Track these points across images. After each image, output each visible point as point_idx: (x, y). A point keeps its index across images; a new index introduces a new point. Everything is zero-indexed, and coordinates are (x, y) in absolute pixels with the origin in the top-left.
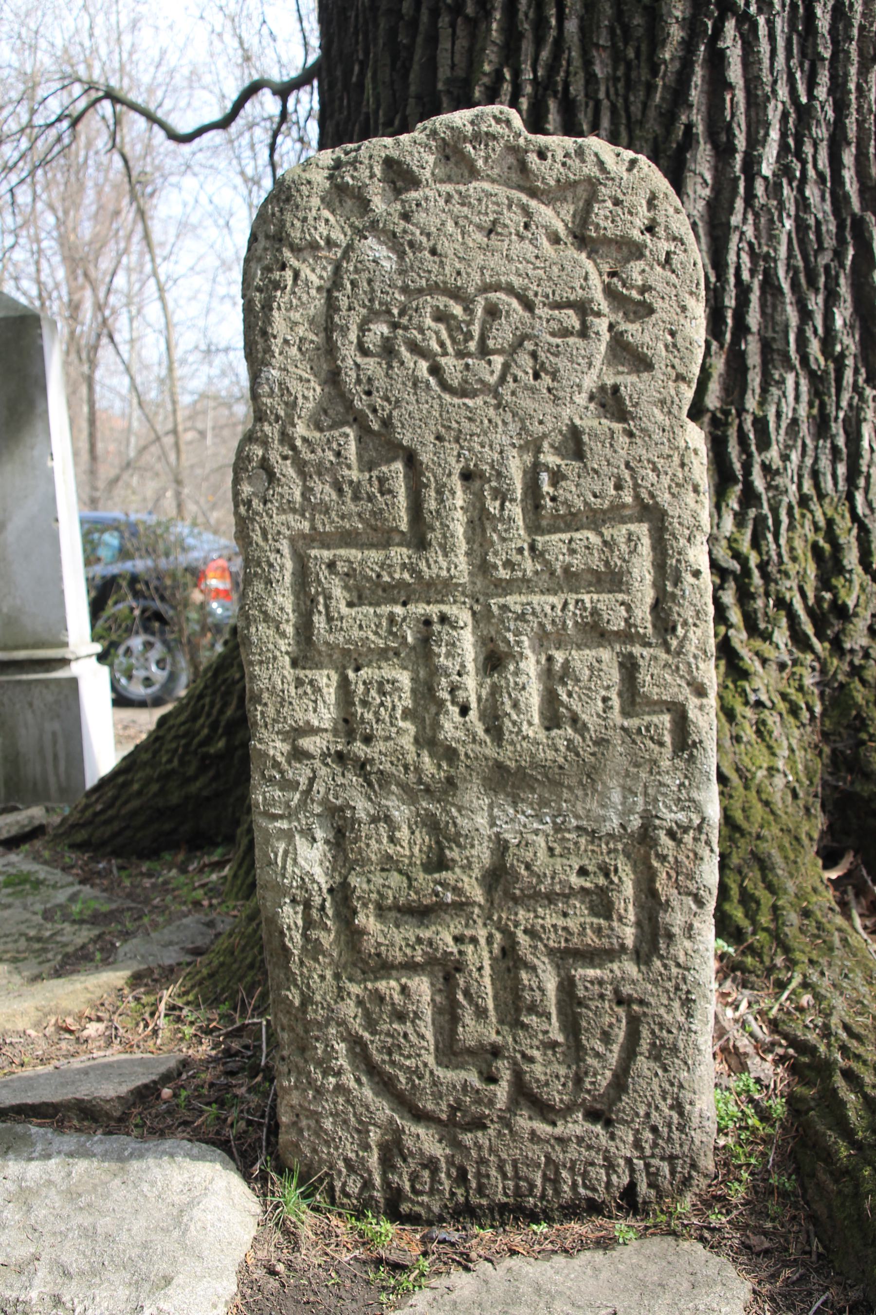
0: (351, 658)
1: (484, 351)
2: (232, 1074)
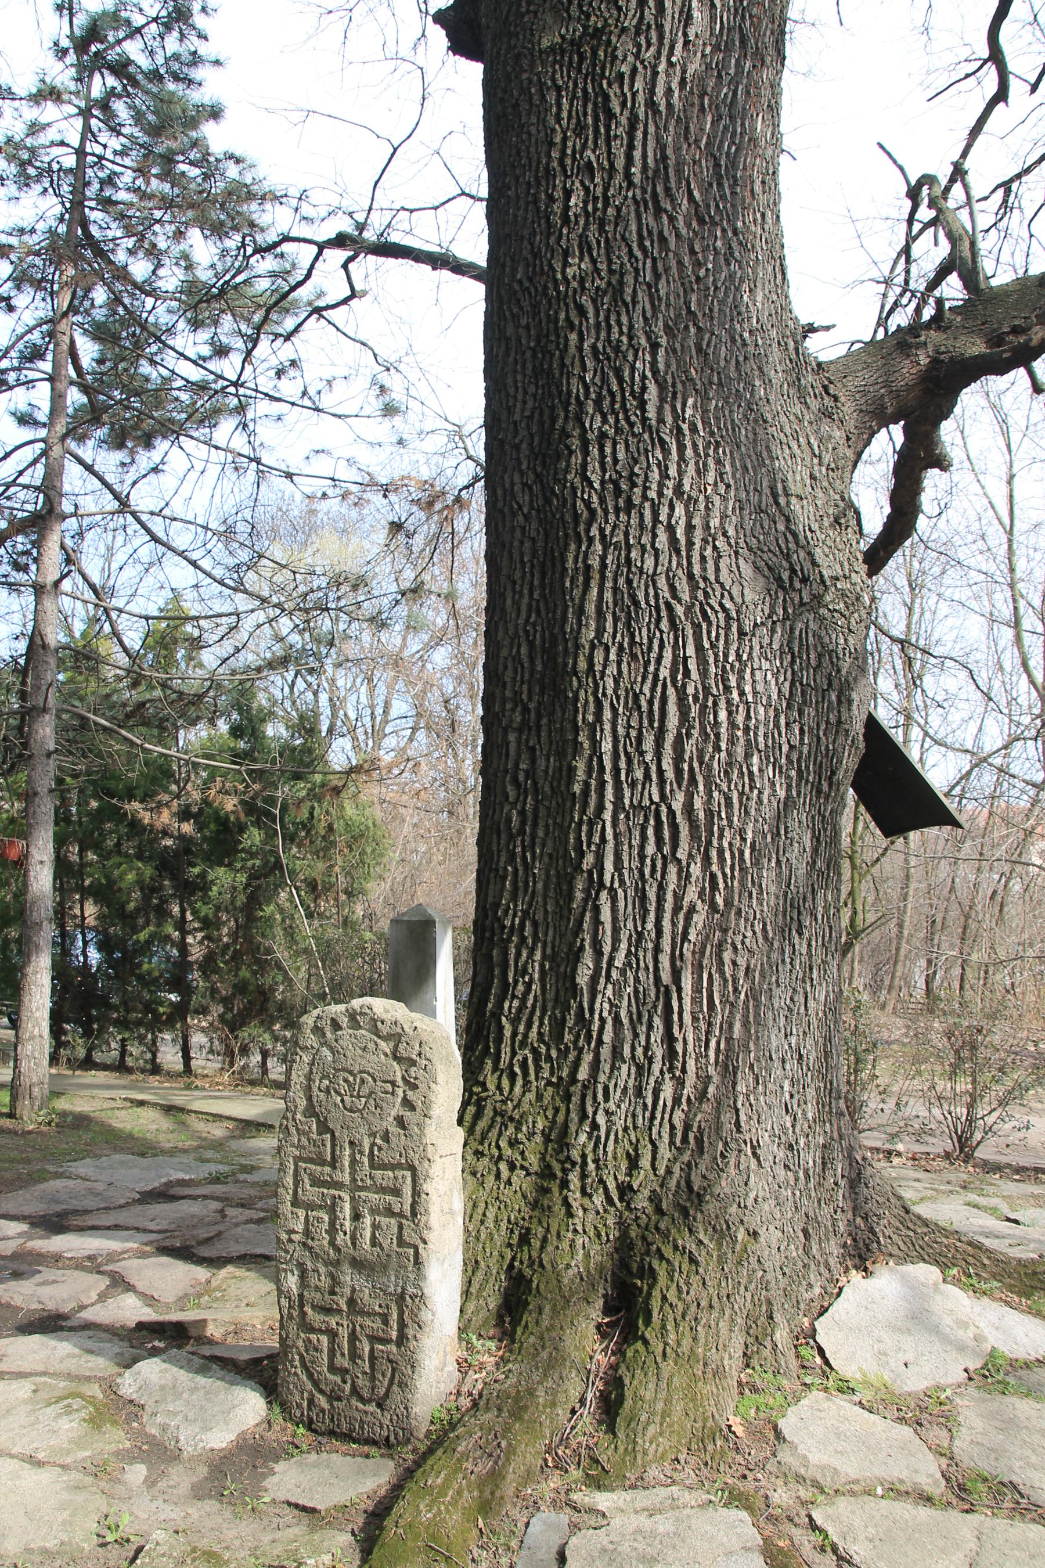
0: (310, 1207)
1: (359, 1096)
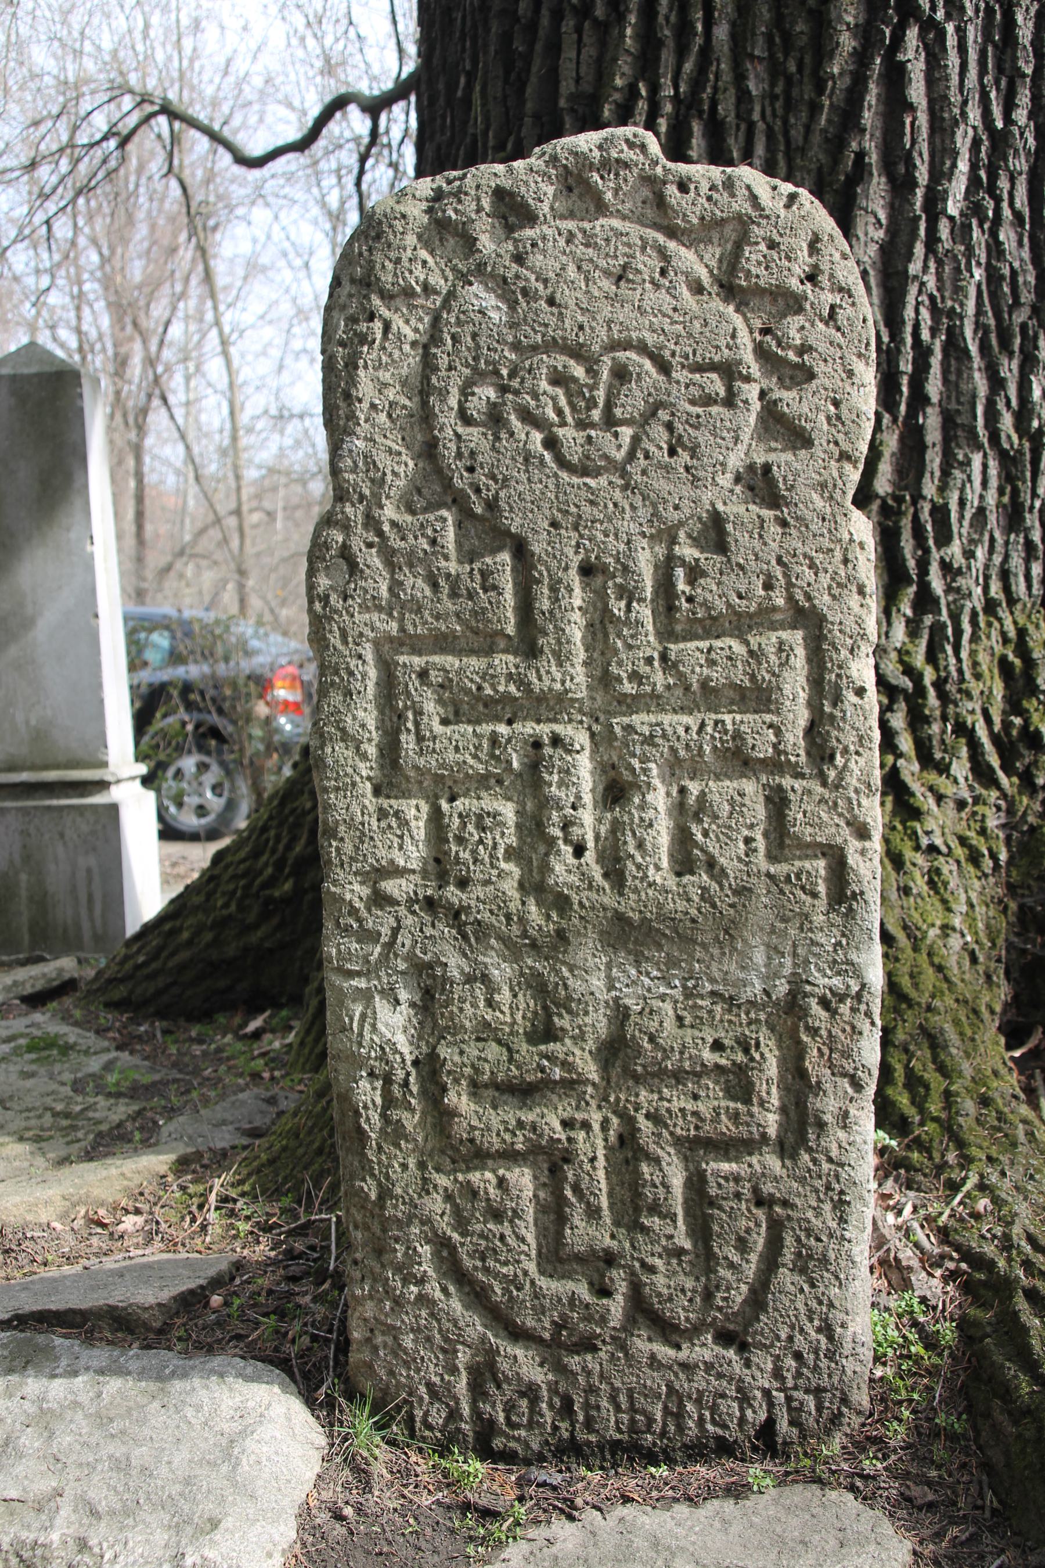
0: (444, 786)
1: (610, 422)
2: (294, 1279)
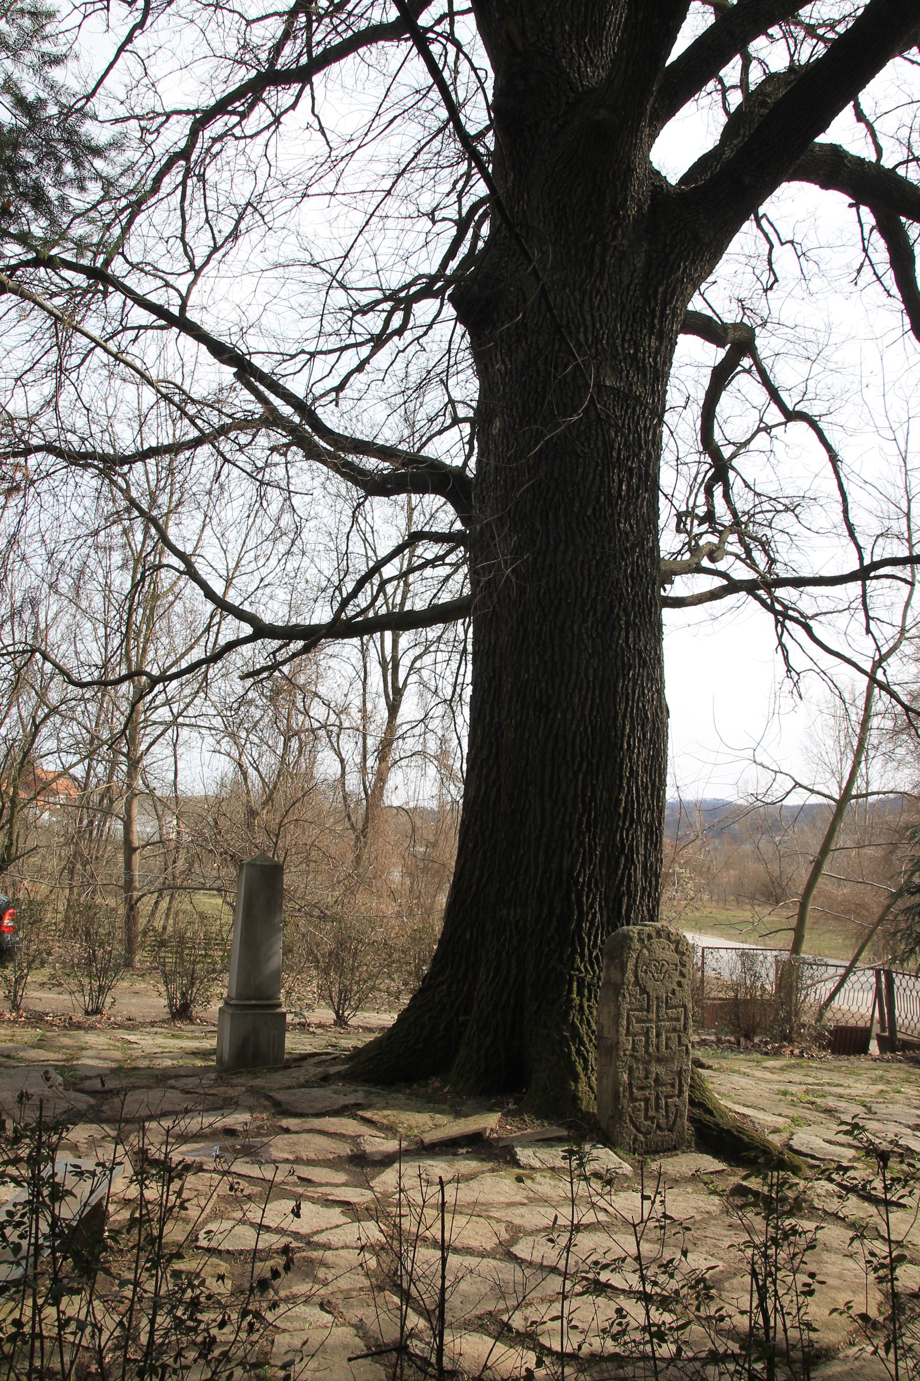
0: (634, 1035)
